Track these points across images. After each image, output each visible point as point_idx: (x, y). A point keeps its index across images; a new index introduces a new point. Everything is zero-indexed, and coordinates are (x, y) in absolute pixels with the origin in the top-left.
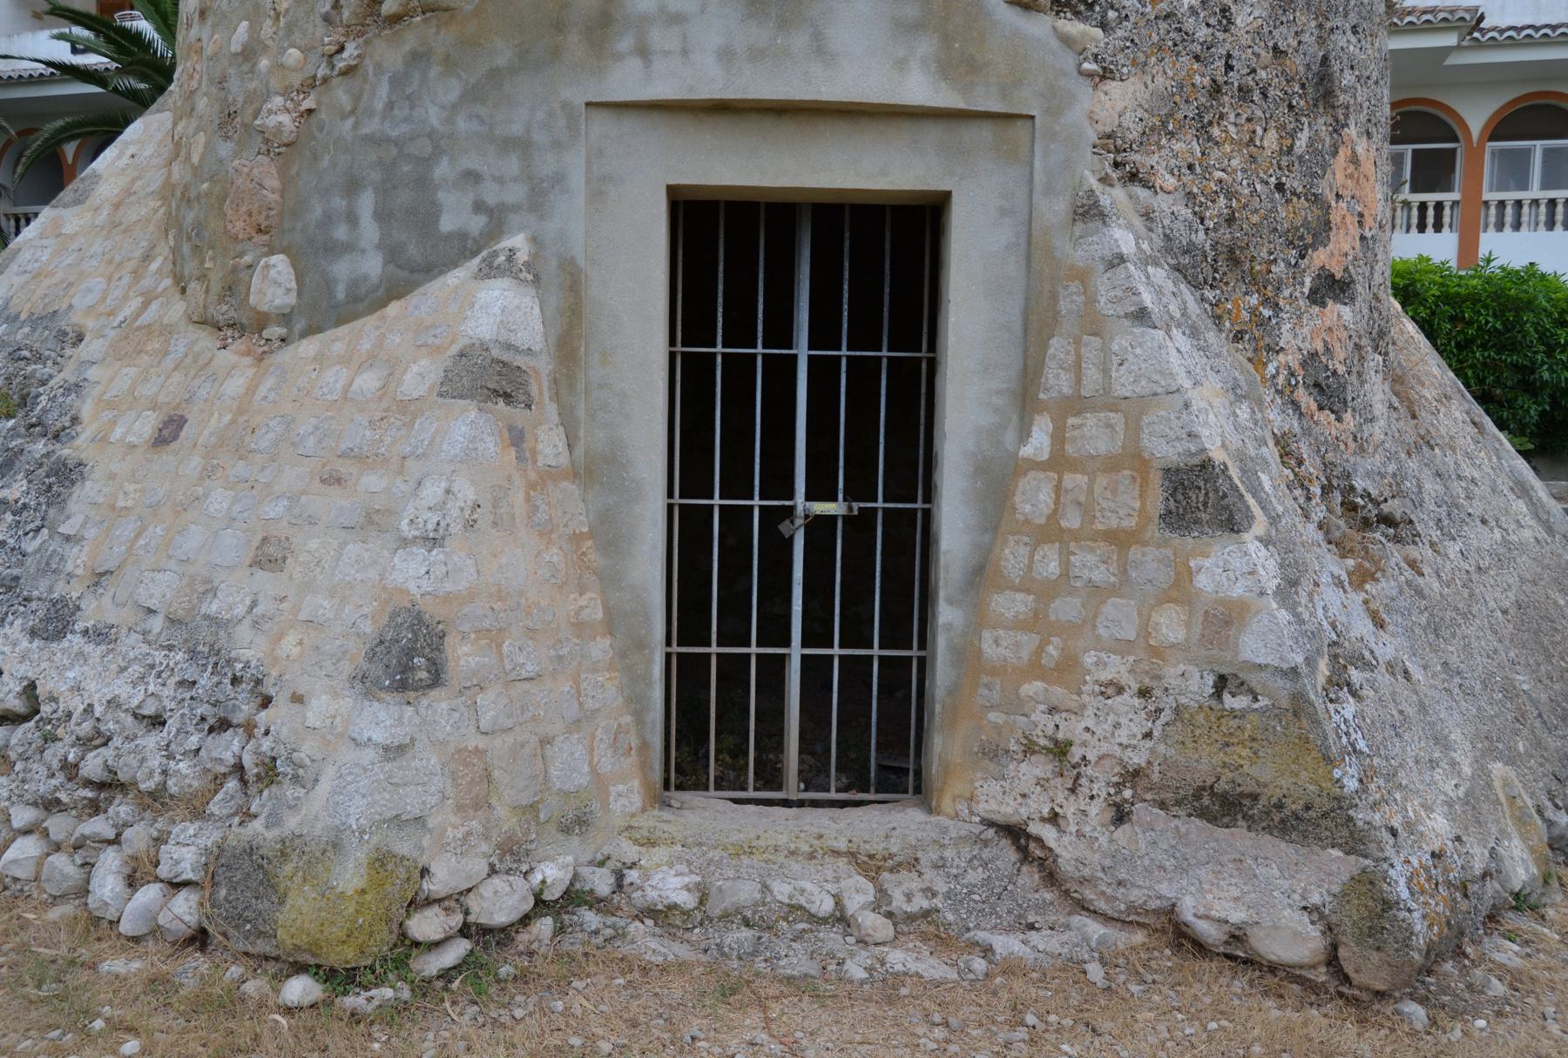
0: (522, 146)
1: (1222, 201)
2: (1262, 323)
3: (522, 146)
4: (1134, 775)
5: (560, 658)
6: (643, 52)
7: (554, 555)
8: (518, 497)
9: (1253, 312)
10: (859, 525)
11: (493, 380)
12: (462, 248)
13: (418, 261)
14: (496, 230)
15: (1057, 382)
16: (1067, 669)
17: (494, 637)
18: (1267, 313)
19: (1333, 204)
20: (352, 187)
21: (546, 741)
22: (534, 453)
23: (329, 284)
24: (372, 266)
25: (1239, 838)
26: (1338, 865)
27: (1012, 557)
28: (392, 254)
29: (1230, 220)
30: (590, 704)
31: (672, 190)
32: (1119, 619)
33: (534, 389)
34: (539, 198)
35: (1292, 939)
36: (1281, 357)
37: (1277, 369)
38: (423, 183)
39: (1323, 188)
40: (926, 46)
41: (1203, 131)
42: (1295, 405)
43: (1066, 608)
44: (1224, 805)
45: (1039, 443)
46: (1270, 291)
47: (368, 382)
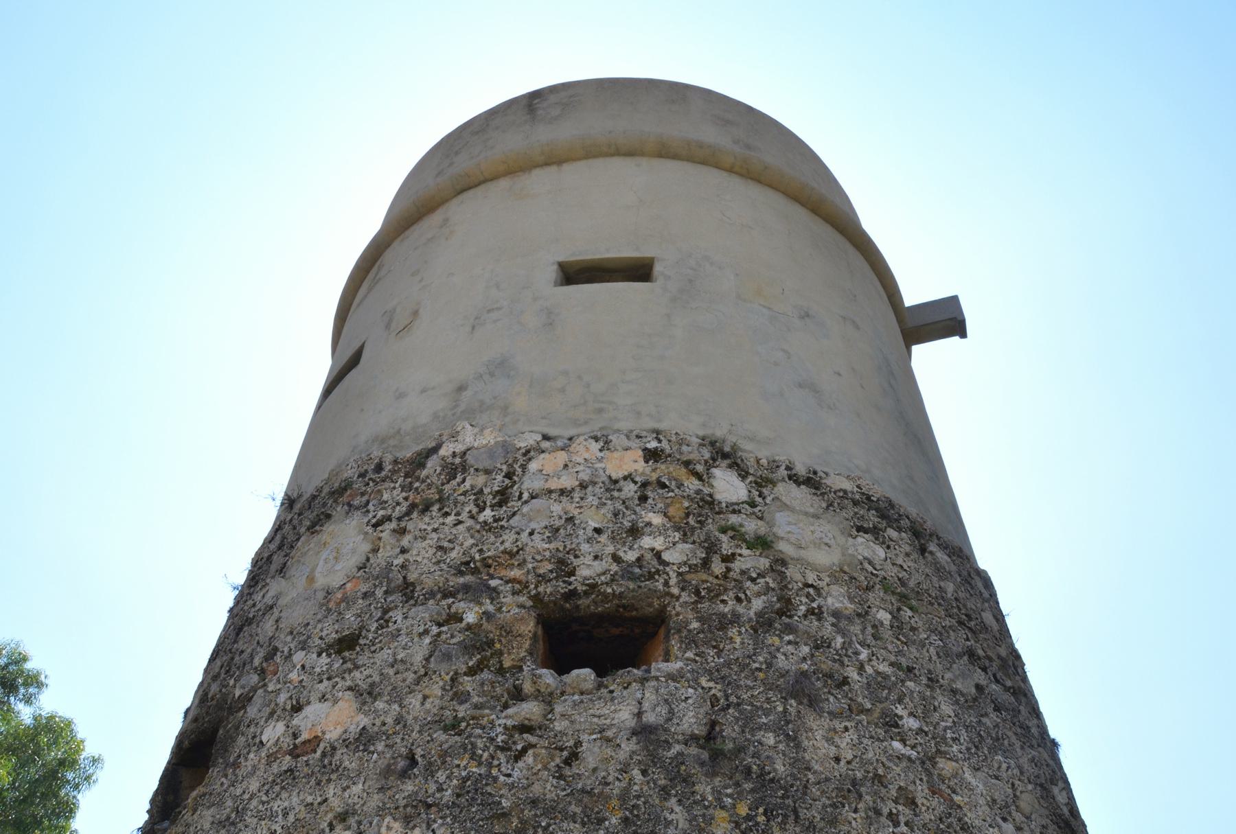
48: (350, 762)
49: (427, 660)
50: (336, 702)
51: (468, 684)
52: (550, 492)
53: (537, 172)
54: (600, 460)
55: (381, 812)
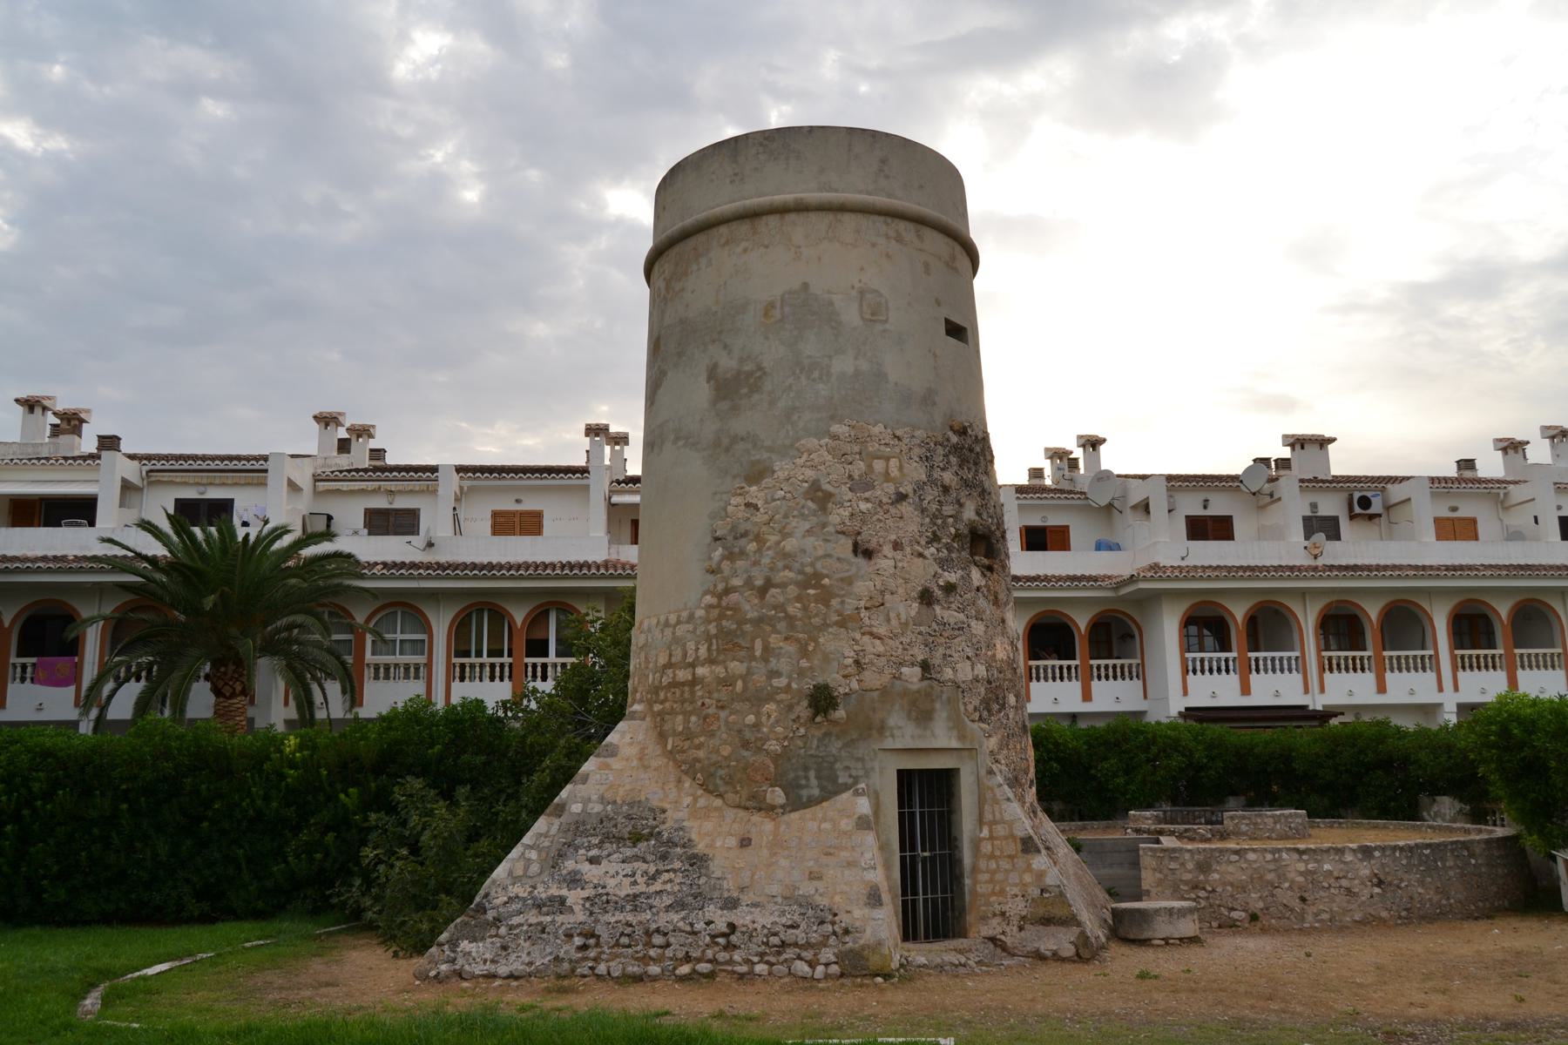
0: (862, 760)
3: (862, 760)
4: (1023, 918)
6: (893, 736)
10: (932, 858)
11: (863, 823)
12: (846, 787)
13: (831, 789)
14: (856, 782)
15: (988, 817)
16: (1002, 892)
20: (806, 769)
23: (800, 797)
24: (816, 792)
25: (1052, 929)
26: (1076, 930)
27: (982, 864)
28: (822, 788)
31: (899, 771)
32: (1014, 877)
34: (867, 775)
35: (1069, 951)
38: (831, 768)
40: (955, 733)
43: (999, 877)
44: (1047, 921)
45: (985, 833)
47: (826, 826)
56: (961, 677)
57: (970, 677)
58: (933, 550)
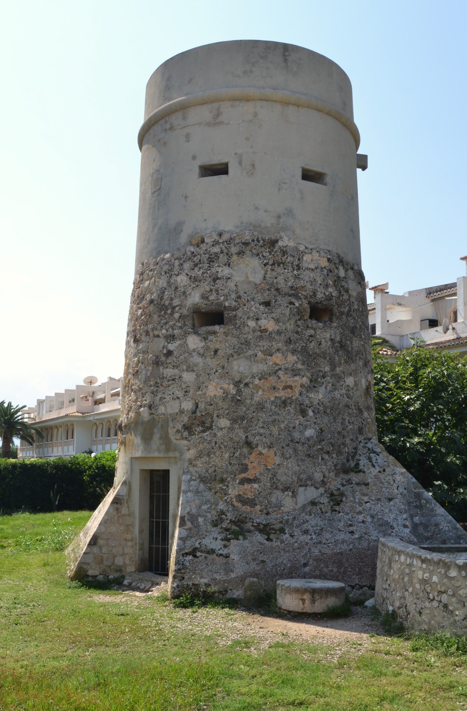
1: (213, 467)
2: (222, 489)
5: (120, 544)
7: (122, 528)
8: (116, 518)
9: (220, 487)
17: (108, 539)
18: (224, 488)
19: (249, 464)
21: (115, 557)
22: (121, 512)
29: (215, 471)
30: (125, 552)
33: (123, 501)
36: (230, 496)
37: (228, 498)
39: (246, 461)
41: (209, 455)
42: (233, 506)
46: (226, 483)
48: (277, 337)
49: (290, 315)
50: (269, 320)
51: (299, 323)
52: (310, 269)
53: (290, 107)
54: (319, 260)
55: (287, 350)
56: (170, 411)
57: (177, 411)
58: (164, 331)
